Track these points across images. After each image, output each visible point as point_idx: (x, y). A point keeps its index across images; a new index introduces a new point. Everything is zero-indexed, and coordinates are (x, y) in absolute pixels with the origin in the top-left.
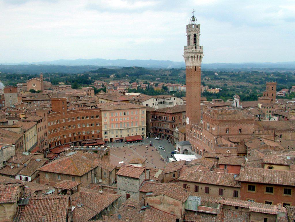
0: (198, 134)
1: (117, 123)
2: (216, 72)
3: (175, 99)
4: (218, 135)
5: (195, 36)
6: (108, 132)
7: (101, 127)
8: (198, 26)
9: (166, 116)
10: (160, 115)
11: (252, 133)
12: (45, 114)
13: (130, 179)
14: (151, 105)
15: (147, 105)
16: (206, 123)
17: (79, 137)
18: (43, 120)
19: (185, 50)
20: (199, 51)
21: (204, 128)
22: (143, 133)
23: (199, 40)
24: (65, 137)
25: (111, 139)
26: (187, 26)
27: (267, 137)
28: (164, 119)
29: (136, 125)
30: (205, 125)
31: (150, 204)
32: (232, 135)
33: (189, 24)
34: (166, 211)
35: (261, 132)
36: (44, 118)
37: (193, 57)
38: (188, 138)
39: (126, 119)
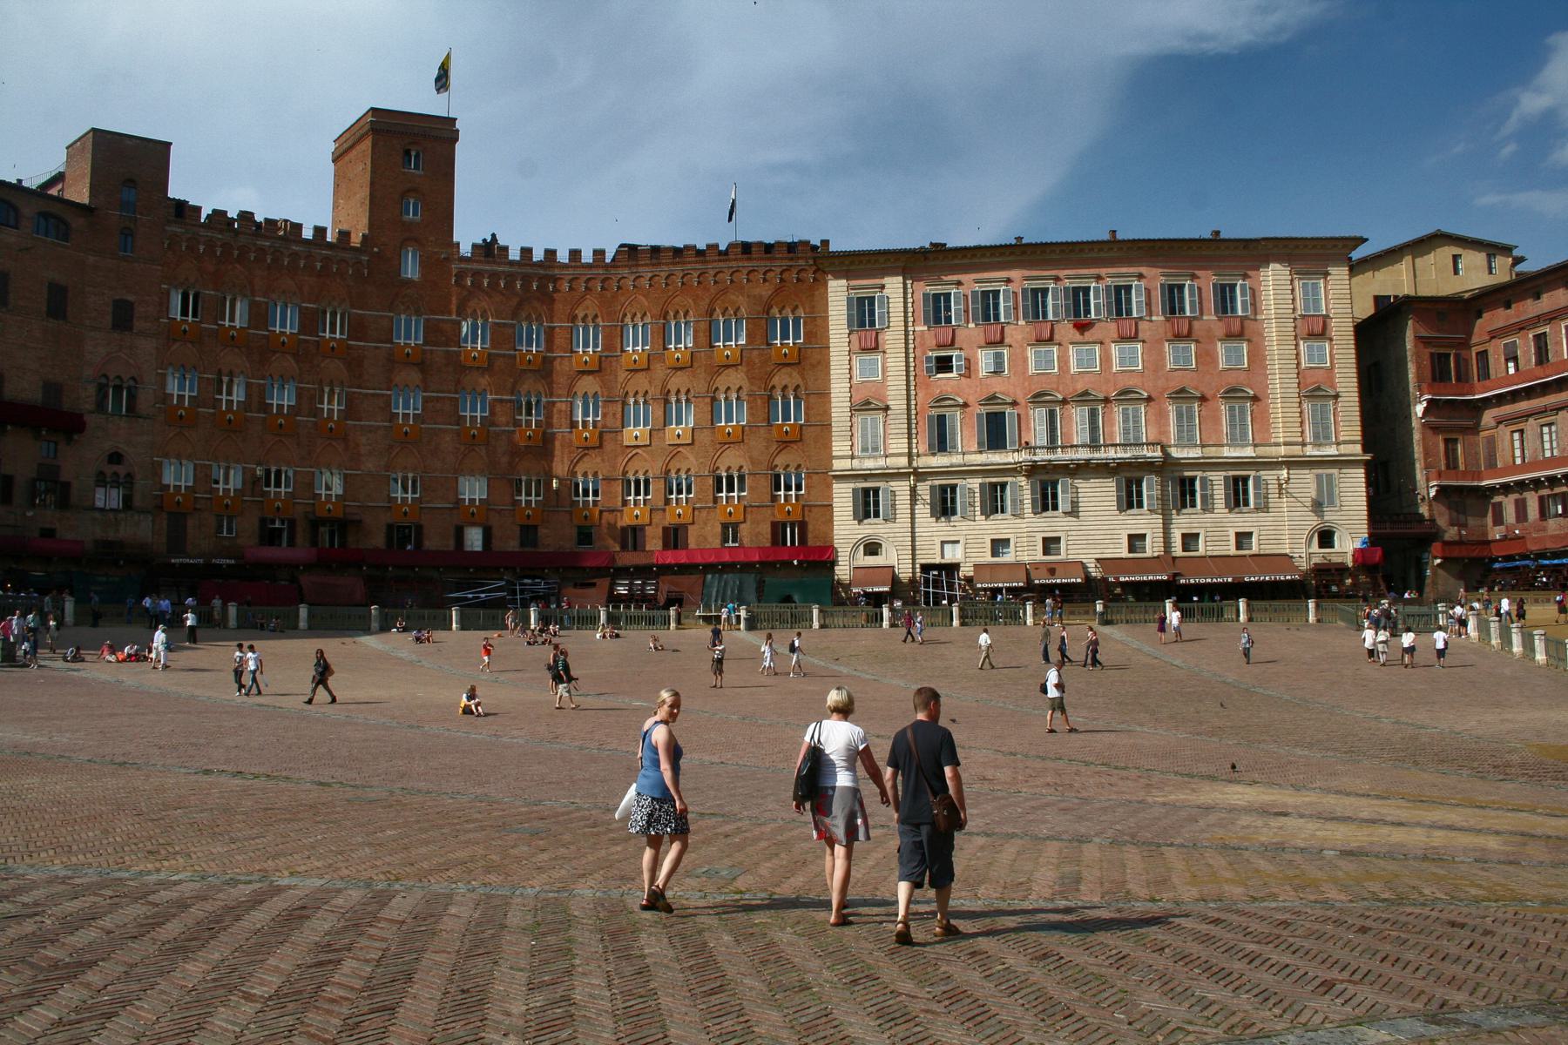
29: (1237, 440)
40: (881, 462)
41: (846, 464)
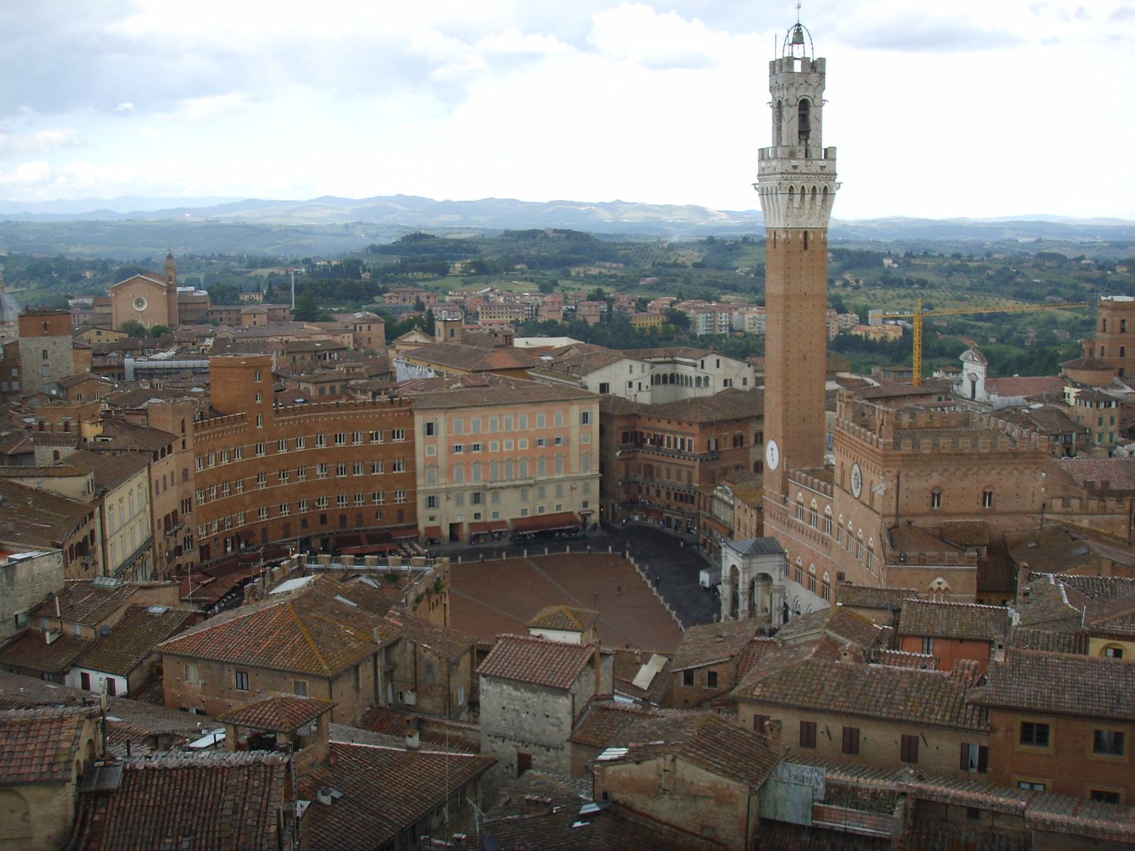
0: (816, 511)
2: (889, 255)
3: (718, 366)
4: (898, 515)
5: (804, 105)
6: (443, 497)
7: (413, 476)
8: (815, 68)
9: (682, 434)
11: (1037, 507)
12: (183, 421)
13: (534, 691)
14: (618, 388)
15: (604, 387)
16: (848, 463)
17: (323, 519)
18: (177, 446)
19: (763, 164)
20: (822, 167)
21: (842, 486)
22: (585, 504)
23: (819, 121)
24: (264, 517)
25: (454, 527)
26: (773, 64)
27: (1097, 524)
28: (675, 447)
29: (559, 471)
30: (843, 473)
31: (617, 796)
32: (955, 515)
33: (779, 56)
34: (683, 826)
35: (1075, 504)
36: (181, 440)
37: (797, 191)
38: (771, 527)
39: (516, 445)
40: (436, 487)
41: (423, 488)
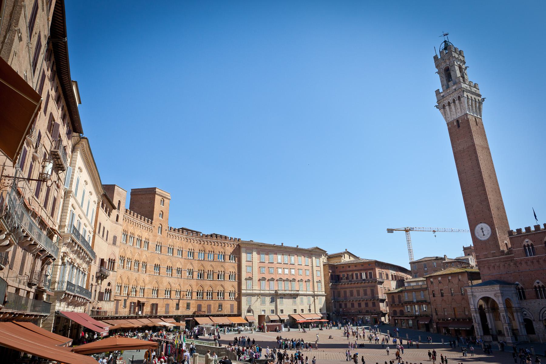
1: (272, 280)
10: (350, 271)
40: (251, 292)
